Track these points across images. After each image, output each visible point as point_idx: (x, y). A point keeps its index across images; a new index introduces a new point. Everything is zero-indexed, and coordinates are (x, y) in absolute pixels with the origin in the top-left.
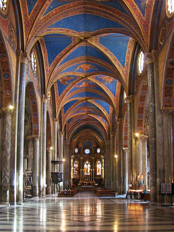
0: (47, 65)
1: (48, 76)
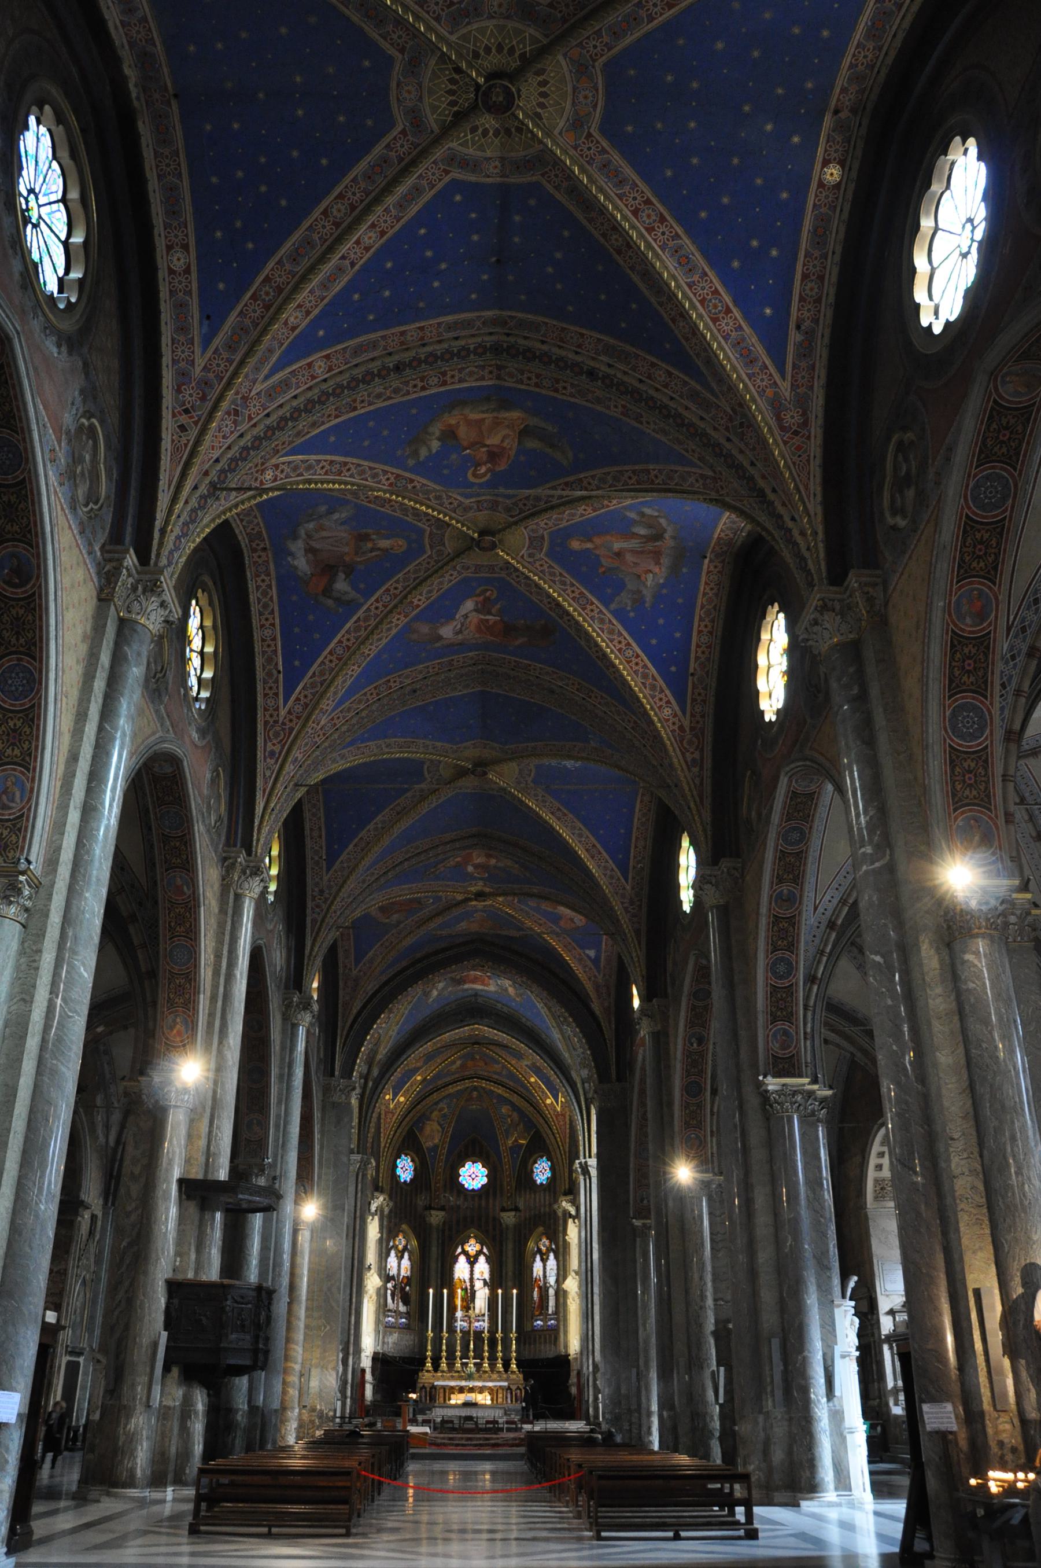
1: (184, 419)
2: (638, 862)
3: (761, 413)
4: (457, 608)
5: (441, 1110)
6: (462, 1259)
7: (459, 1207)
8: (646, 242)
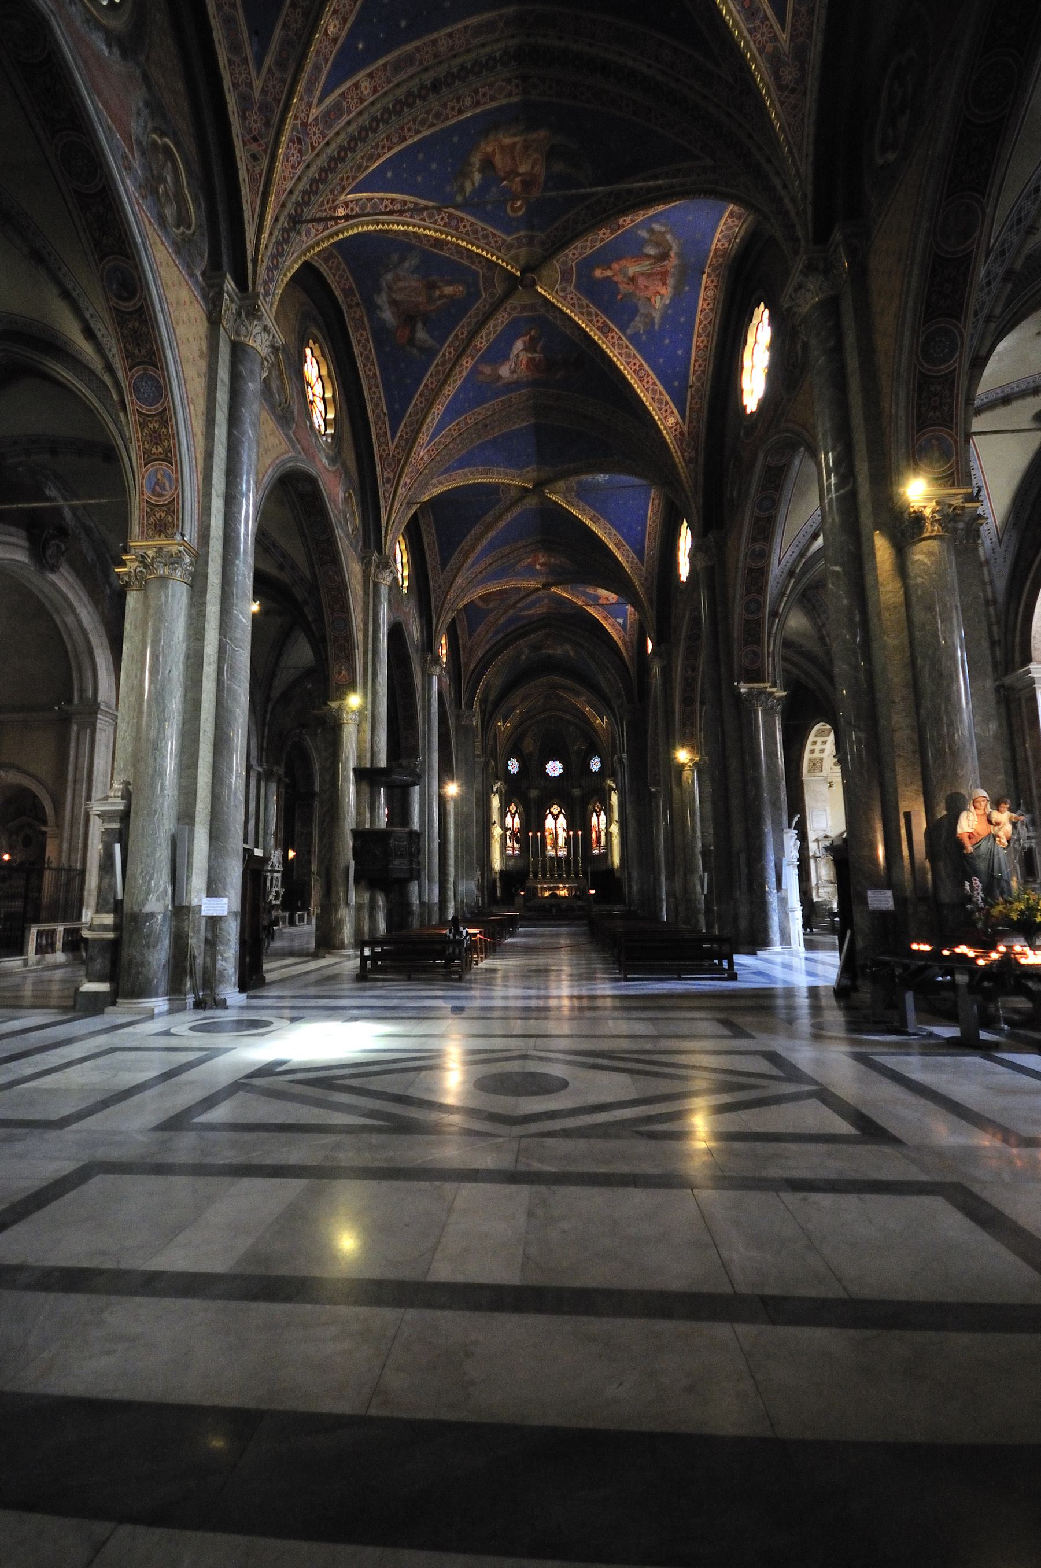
0: (235, 48)
1: (254, 146)
2: (651, 550)
4: (511, 348)
6: (550, 817)
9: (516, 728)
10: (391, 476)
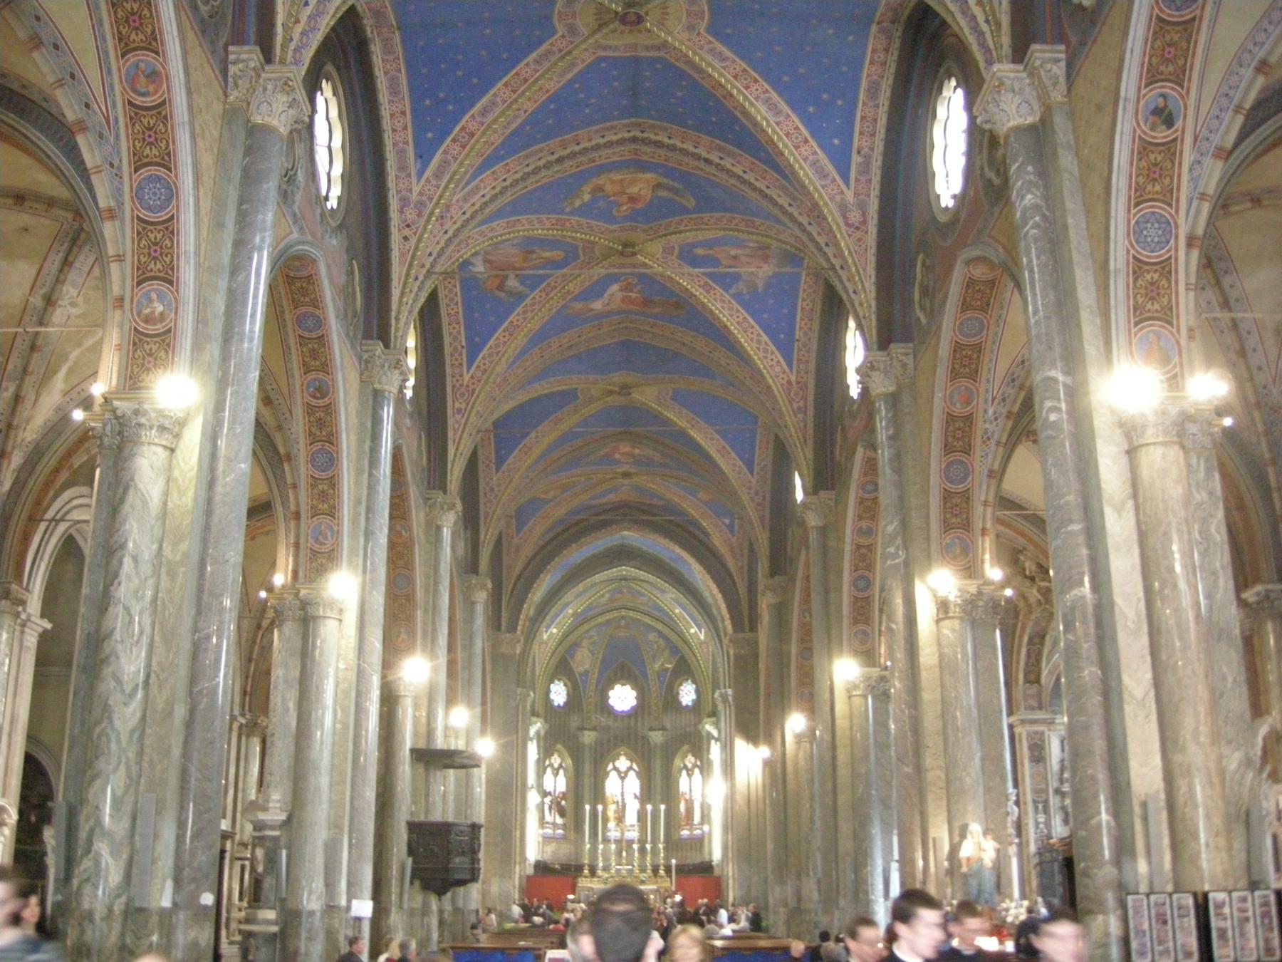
0: (402, 168)
1: (407, 232)
3: (832, 214)
4: (605, 291)
5: (591, 637)
6: (613, 775)
7: (609, 727)
8: (745, 97)
9: (567, 635)
10: (463, 406)
